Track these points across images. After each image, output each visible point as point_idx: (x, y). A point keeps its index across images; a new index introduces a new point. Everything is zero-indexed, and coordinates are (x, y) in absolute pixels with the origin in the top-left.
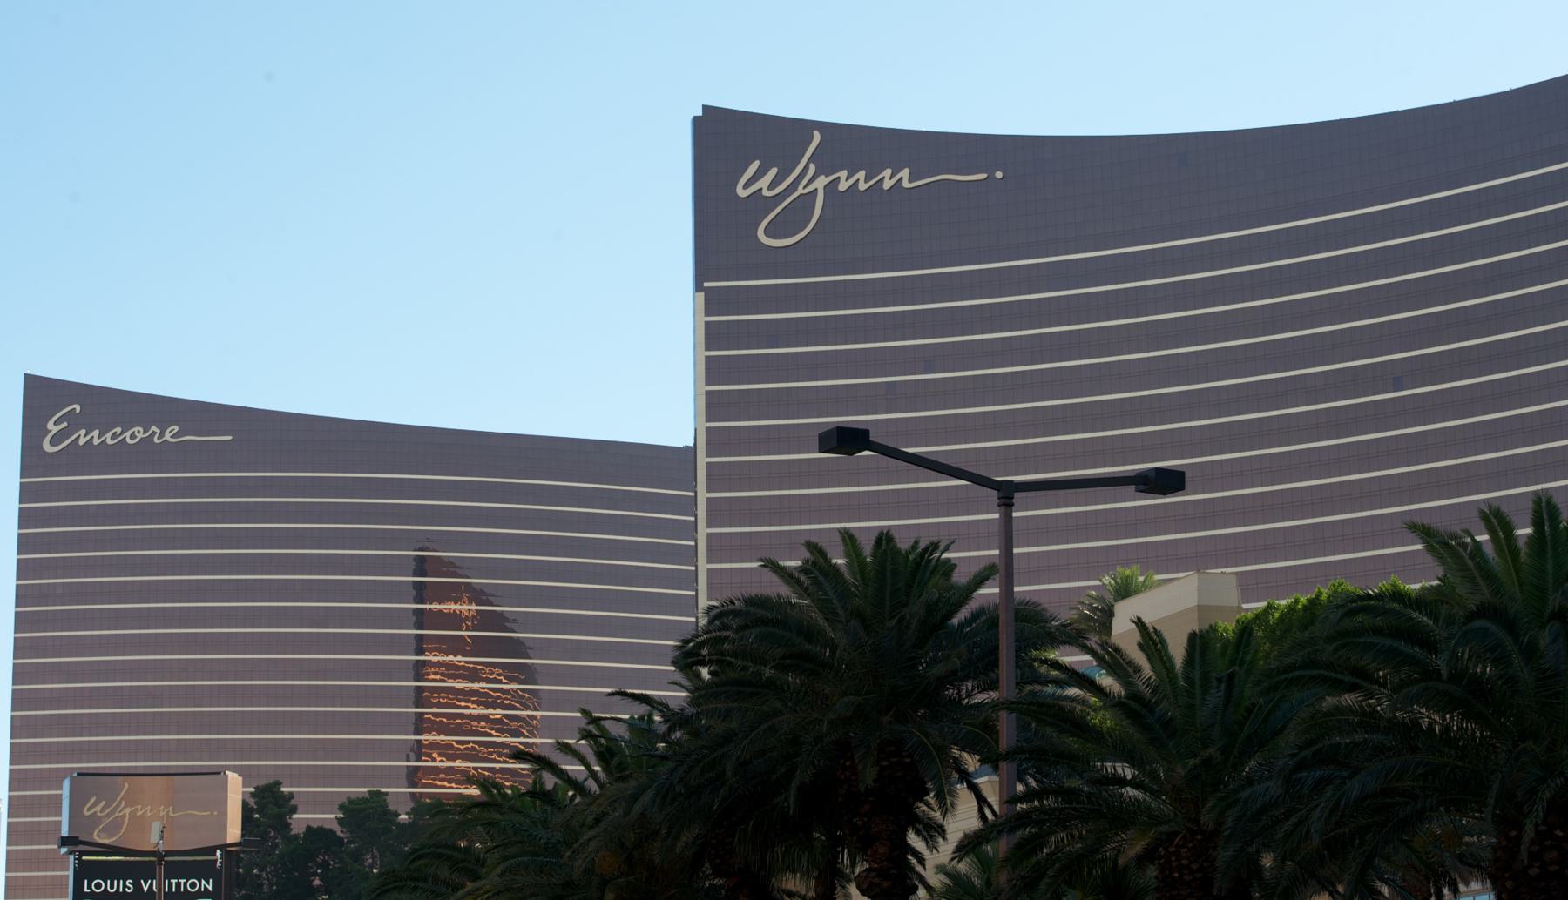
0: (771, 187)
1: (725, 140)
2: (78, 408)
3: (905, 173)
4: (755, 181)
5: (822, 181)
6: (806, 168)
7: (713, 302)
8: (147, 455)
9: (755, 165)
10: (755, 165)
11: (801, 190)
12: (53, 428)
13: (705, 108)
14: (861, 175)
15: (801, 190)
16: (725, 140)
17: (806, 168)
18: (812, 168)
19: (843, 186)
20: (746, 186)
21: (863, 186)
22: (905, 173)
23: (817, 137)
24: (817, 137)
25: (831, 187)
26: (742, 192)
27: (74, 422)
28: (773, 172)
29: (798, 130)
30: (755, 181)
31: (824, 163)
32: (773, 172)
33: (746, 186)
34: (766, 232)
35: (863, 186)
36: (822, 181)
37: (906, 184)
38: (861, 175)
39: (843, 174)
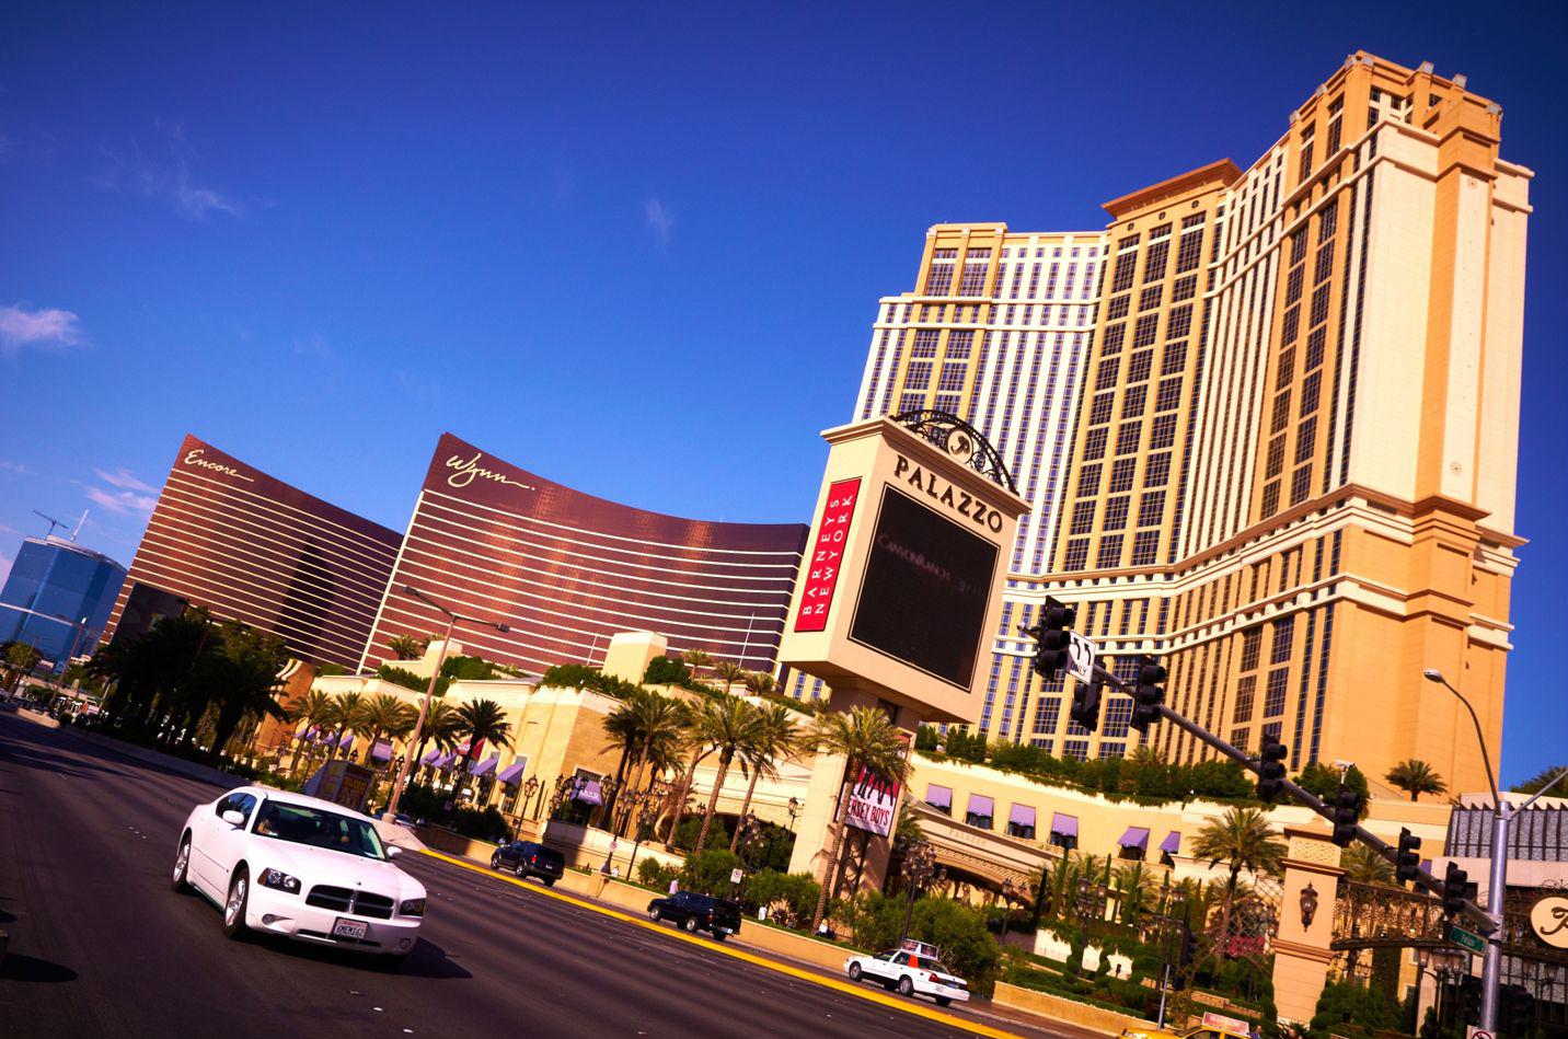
1: (450, 446)
2: (202, 452)
3: (503, 477)
4: (454, 462)
5: (476, 470)
7: (427, 497)
8: (221, 476)
9: (456, 457)
10: (456, 457)
12: (191, 455)
13: (447, 434)
14: (489, 473)
16: (450, 446)
19: (482, 474)
21: (488, 477)
22: (503, 477)
23: (480, 455)
24: (480, 455)
25: (478, 473)
26: (448, 464)
27: (200, 456)
29: (475, 451)
30: (454, 462)
31: (479, 465)
34: (453, 480)
35: (488, 477)
36: (476, 470)
38: (489, 473)
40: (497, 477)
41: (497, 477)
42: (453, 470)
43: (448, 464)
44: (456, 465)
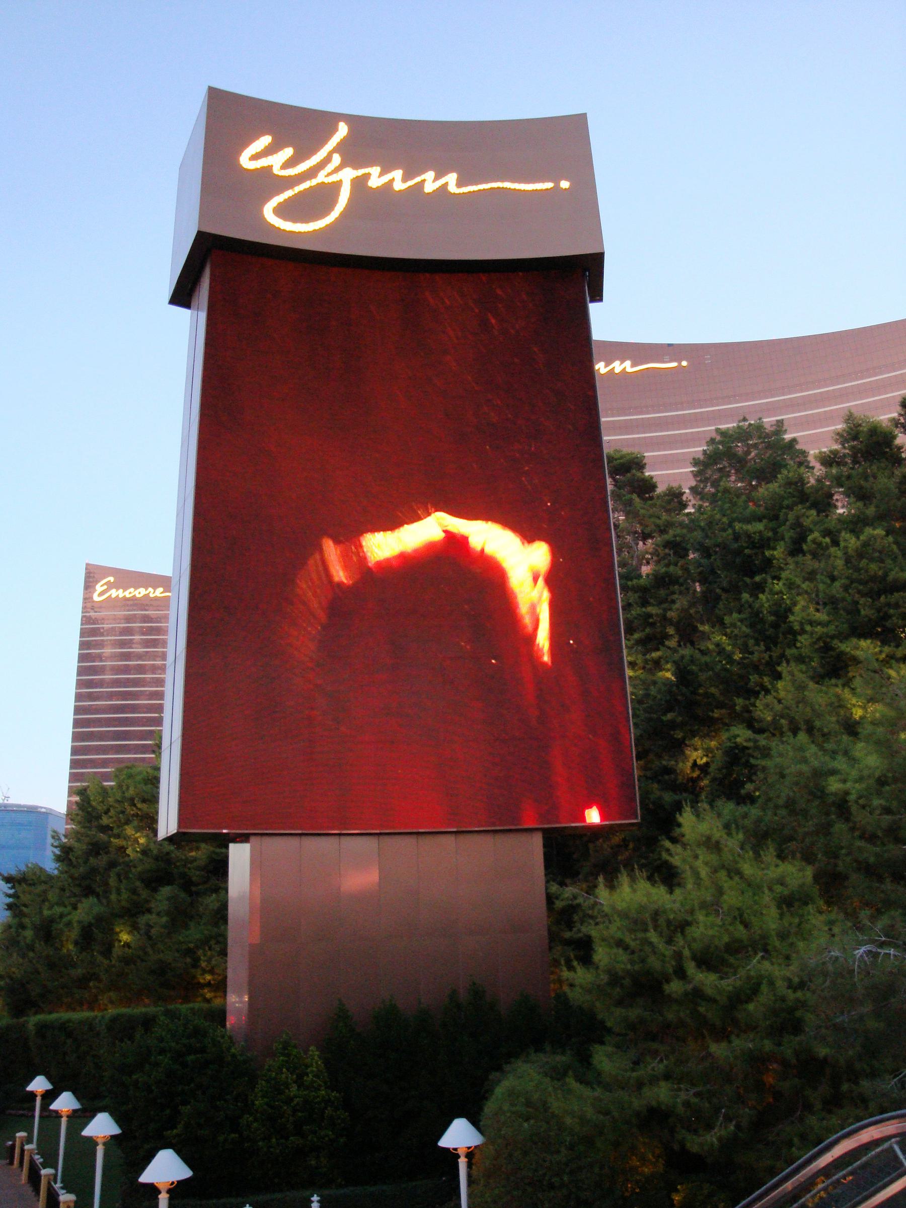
0: (285, 166)
3: (451, 179)
6: (328, 160)
10: (265, 141)
11: (321, 177)
14: (397, 174)
15: (321, 177)
17: (328, 160)
18: (337, 159)
19: (376, 181)
20: (255, 157)
22: (451, 179)
23: (343, 130)
24: (343, 130)
25: (359, 184)
28: (288, 152)
29: (323, 123)
31: (352, 153)
32: (288, 152)
33: (255, 157)
34: (278, 211)
36: (348, 175)
37: (453, 189)
38: (397, 174)
39: (375, 171)
40: (430, 182)
41: (430, 182)
42: (267, 183)
43: (246, 161)
44: (276, 161)
